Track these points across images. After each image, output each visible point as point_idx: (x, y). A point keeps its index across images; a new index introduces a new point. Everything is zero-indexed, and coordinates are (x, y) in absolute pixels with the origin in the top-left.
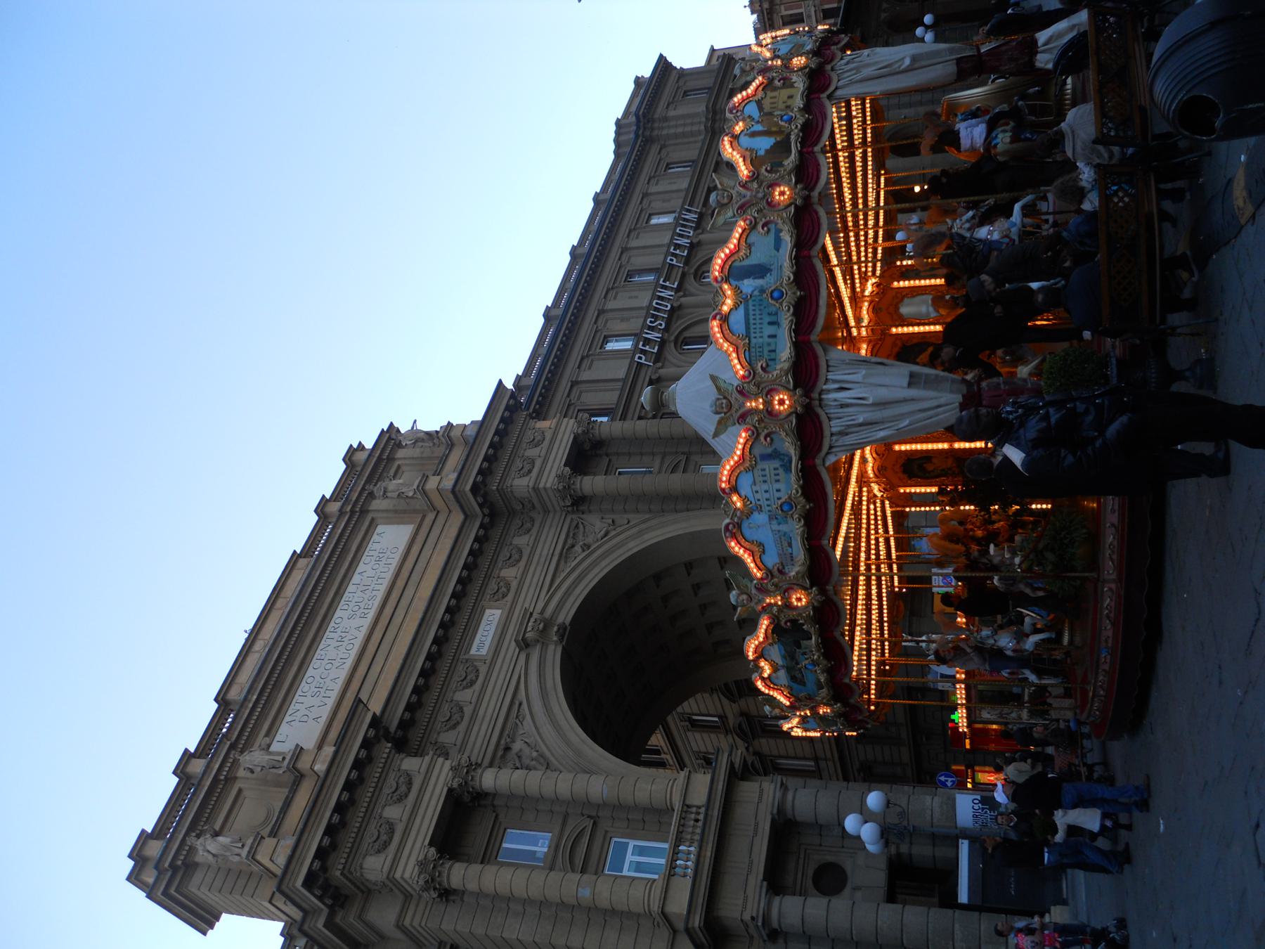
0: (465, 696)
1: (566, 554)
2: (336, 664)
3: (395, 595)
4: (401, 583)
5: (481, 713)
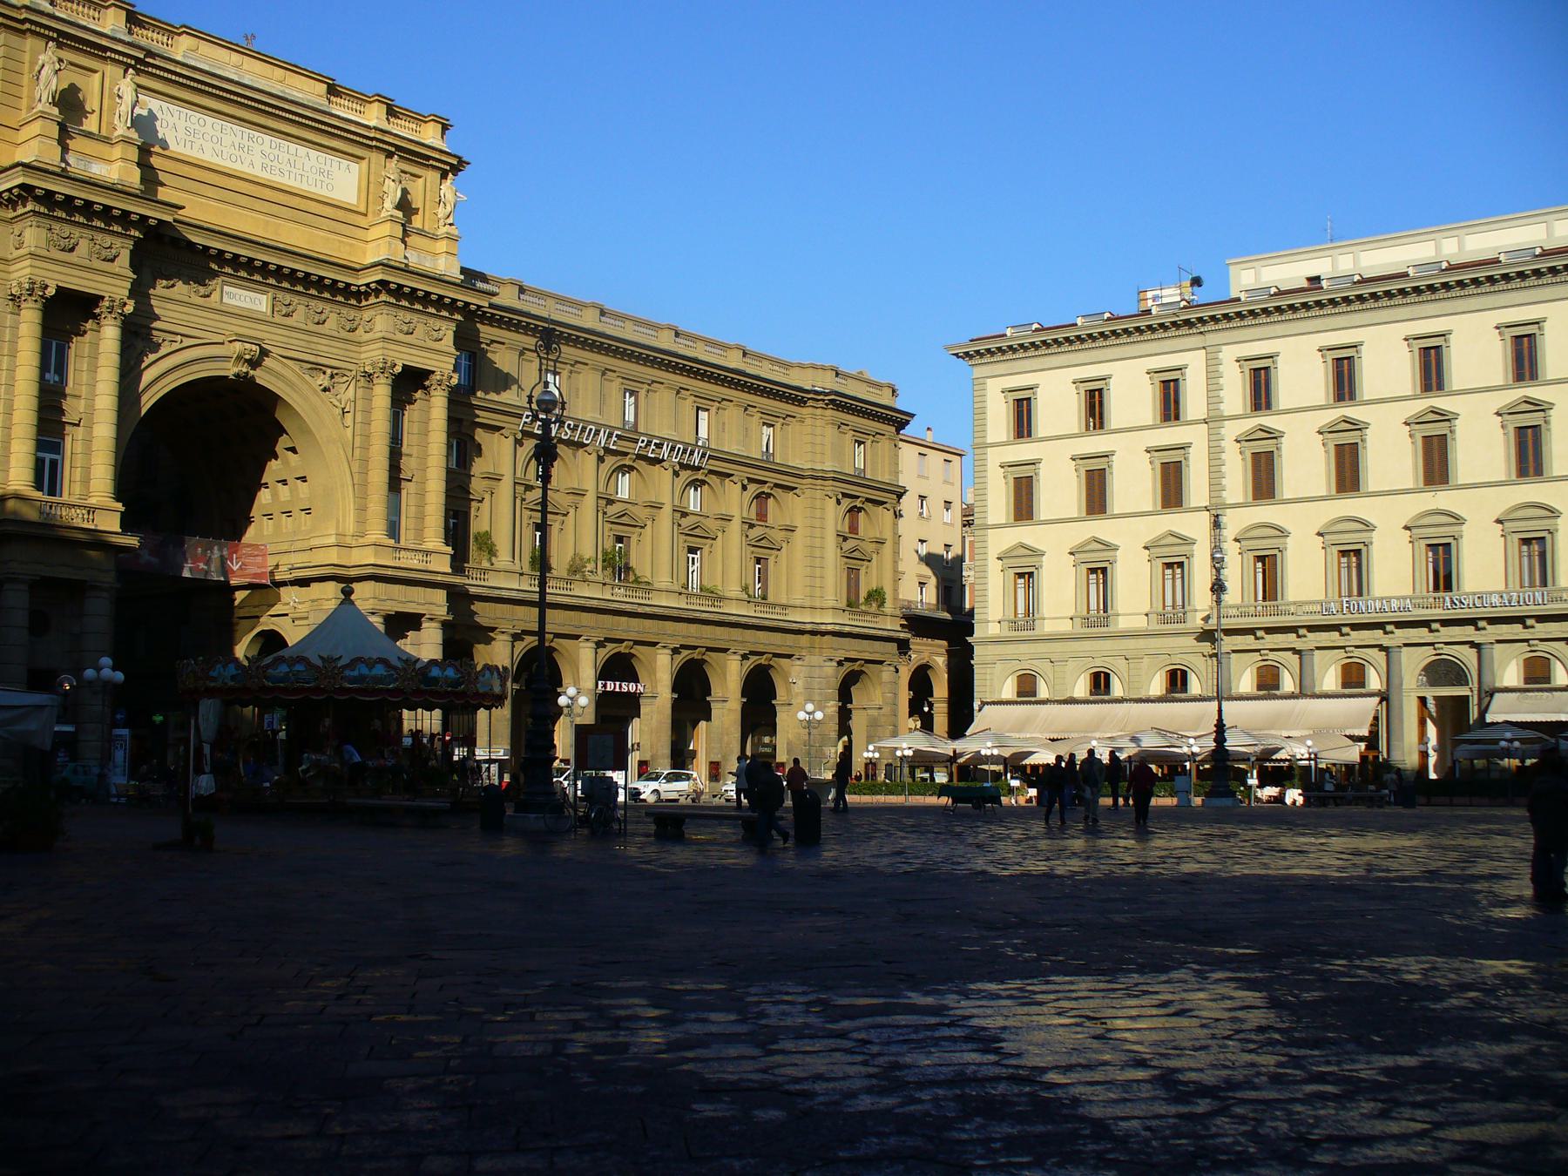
4: (295, 202)
5: (169, 306)
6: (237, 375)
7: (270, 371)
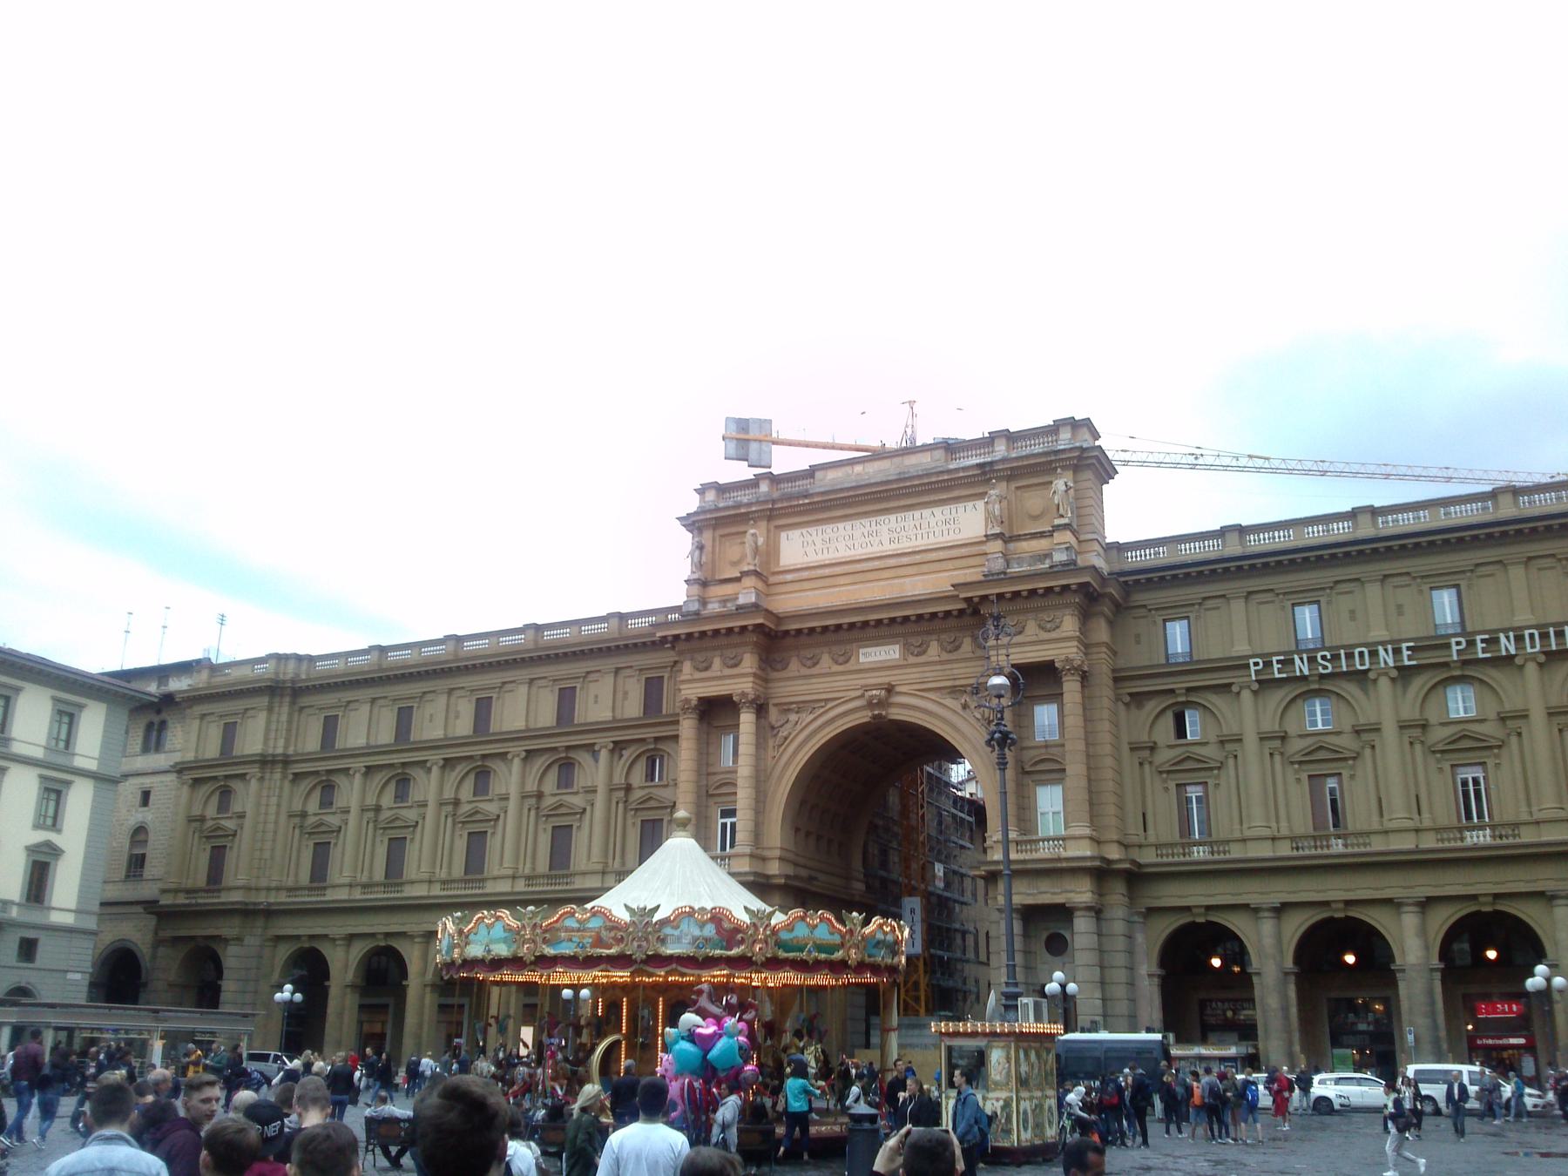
0: (826, 662)
1: (954, 691)
2: (850, 543)
3: (905, 560)
4: (918, 558)
6: (874, 717)
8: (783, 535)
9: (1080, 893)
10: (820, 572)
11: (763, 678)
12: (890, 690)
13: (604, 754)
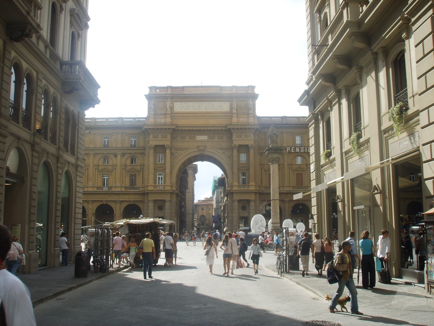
0: (187, 138)
1: (221, 149)
3: (210, 115)
7: (209, 151)
8: (175, 103)
9: (252, 197)
10: (186, 115)
11: (171, 142)
12: (205, 147)
13: (119, 157)
